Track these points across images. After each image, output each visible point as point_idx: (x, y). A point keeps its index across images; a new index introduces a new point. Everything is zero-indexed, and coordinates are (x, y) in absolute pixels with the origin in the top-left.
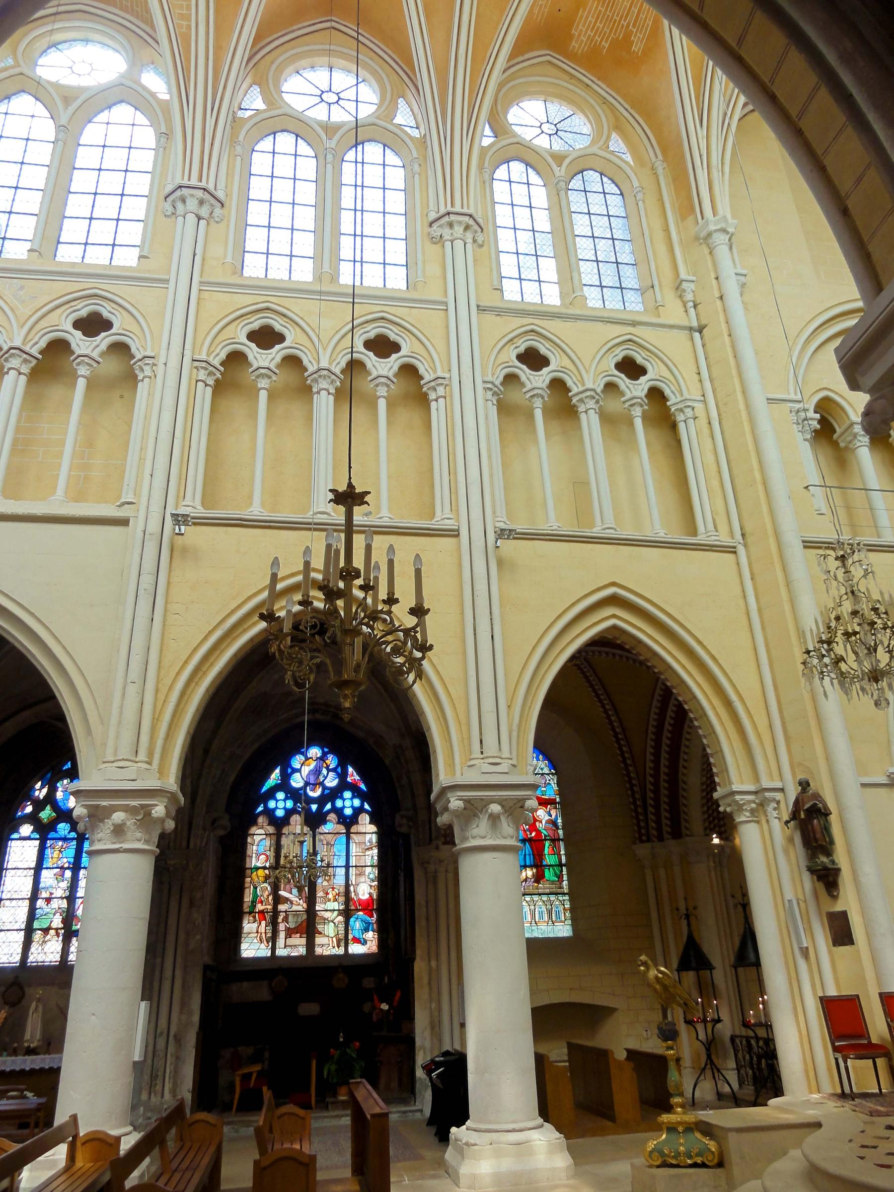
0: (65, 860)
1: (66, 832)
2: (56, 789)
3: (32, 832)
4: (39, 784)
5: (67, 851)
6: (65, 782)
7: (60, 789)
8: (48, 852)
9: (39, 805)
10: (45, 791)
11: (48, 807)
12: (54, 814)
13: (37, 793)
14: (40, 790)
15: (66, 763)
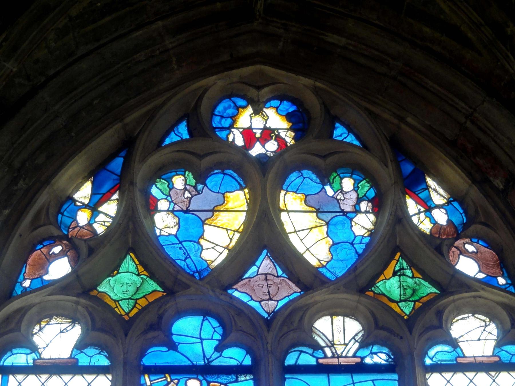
1: (209, 346)
2: (151, 206)
3: (81, 346)
4: (84, 193)
6: (178, 182)
7: (163, 205)
9: (94, 255)
10: (110, 208)
11: (129, 264)
12: (151, 286)
13: (83, 217)
14: (94, 208)
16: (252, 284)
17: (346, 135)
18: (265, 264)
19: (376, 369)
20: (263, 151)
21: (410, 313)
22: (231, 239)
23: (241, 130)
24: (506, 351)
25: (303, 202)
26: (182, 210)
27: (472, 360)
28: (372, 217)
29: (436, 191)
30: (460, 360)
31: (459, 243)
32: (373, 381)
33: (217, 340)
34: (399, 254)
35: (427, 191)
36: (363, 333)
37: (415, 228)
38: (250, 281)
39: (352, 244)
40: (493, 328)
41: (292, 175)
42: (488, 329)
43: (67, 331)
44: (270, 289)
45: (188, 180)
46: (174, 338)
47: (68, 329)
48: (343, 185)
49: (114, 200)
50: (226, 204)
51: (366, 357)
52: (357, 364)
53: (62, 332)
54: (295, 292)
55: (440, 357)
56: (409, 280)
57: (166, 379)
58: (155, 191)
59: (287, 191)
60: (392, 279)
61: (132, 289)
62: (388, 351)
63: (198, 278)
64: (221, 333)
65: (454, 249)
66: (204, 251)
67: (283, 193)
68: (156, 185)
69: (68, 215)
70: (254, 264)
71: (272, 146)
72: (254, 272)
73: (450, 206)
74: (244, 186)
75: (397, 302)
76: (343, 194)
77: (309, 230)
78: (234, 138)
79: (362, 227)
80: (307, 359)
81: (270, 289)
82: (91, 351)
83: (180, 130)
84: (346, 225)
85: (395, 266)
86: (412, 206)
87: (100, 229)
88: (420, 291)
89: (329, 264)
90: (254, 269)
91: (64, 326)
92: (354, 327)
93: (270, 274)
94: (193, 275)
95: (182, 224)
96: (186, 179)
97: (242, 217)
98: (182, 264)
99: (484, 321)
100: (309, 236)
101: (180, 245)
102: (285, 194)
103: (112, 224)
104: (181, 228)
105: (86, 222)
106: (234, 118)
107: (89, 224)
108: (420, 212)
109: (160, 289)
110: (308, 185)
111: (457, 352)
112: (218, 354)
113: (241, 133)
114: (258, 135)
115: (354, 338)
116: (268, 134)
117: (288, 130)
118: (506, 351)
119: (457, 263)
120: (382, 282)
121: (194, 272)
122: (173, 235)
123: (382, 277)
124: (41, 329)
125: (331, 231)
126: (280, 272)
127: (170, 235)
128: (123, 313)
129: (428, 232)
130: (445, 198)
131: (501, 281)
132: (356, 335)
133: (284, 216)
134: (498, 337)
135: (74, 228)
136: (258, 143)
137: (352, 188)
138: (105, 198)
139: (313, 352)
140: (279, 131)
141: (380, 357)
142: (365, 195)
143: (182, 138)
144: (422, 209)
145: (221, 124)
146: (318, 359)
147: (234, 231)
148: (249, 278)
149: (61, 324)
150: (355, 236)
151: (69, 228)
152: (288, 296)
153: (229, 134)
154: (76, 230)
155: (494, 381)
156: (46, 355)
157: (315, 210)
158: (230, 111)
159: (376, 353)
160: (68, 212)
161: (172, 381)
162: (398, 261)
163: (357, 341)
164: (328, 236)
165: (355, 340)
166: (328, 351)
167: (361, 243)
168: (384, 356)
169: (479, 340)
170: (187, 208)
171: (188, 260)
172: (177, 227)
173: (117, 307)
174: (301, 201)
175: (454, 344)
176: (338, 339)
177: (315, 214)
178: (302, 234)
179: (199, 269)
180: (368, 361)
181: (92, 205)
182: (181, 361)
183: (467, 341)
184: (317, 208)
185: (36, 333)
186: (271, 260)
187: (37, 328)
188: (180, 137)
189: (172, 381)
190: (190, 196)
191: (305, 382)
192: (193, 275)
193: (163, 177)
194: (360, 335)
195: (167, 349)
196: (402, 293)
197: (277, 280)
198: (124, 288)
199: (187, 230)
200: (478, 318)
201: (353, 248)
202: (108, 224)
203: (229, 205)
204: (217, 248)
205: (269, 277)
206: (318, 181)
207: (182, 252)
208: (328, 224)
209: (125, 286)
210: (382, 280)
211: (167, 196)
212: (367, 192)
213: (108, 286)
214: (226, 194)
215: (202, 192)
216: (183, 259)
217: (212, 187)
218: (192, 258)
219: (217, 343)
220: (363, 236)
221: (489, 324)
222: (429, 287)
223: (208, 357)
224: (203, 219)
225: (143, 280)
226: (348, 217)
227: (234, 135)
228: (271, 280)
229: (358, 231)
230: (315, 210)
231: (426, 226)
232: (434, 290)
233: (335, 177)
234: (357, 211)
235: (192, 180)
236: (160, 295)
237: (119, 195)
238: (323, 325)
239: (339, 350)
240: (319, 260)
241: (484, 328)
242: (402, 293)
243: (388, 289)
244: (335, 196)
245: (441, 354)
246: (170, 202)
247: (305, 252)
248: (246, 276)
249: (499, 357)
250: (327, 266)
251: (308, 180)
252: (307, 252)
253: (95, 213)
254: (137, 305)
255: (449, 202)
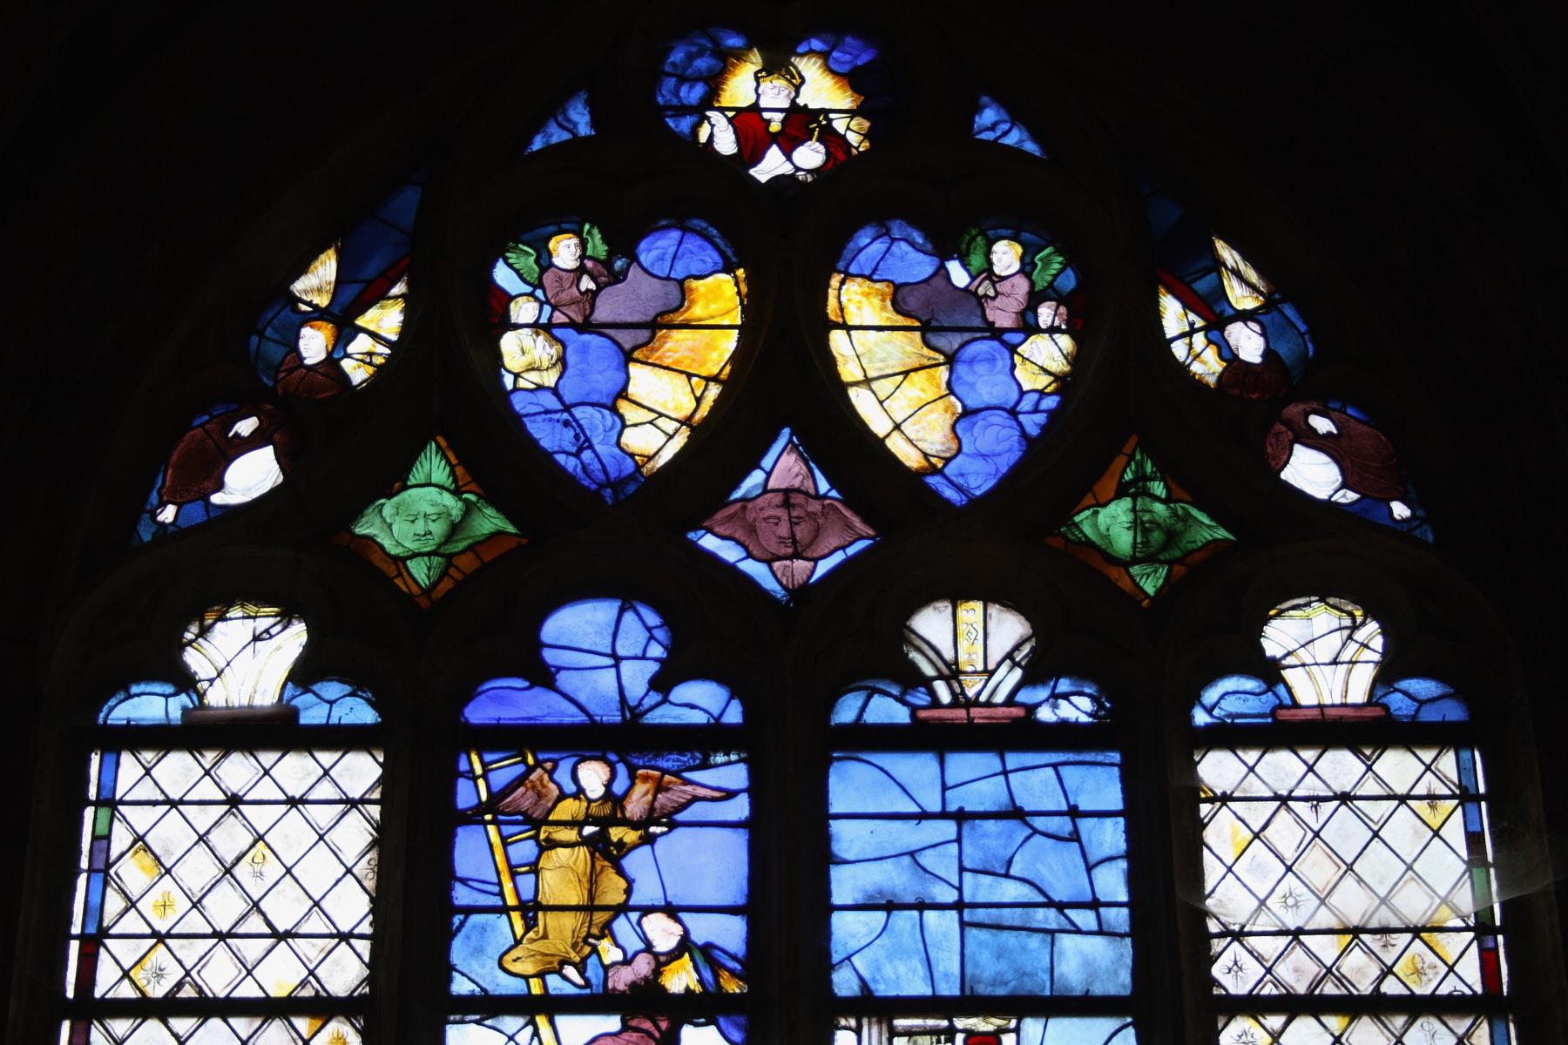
0: (663, 932)
1: (637, 677)
3: (304, 675)
4: (319, 279)
5: (675, 845)
6: (565, 251)
7: (524, 311)
8: (474, 853)
9: (344, 444)
10: (386, 319)
11: (433, 466)
12: (490, 521)
13: (314, 344)
15: (553, 109)
16: (750, 516)
17: (1006, 127)
18: (782, 465)
19: (1064, 737)
20: (787, 169)
21: (1158, 592)
22: (699, 400)
23: (730, 114)
24: (1405, 693)
25: (888, 303)
26: (572, 325)
27: (1316, 712)
28: (1066, 342)
29: (1237, 273)
30: (1284, 715)
31: (1293, 410)
32: (1055, 766)
33: (656, 660)
34: (1133, 440)
35: (1214, 275)
36: (1033, 642)
37: (1183, 369)
38: (744, 508)
39: (1013, 413)
40: (1371, 631)
41: (861, 233)
42: (1360, 635)
43: (271, 637)
44: (797, 529)
45: (589, 246)
46: (550, 656)
47: (273, 631)
48: (994, 258)
49: (396, 297)
50: (689, 308)
51: (1039, 705)
52: (1016, 720)
53: (256, 638)
54: (861, 538)
55: (1231, 705)
56: (1159, 508)
57: (524, 761)
58: (503, 276)
59: (848, 276)
60: (1113, 506)
61: (439, 529)
62: (1098, 691)
63: (609, 501)
64: (666, 641)
65: (1279, 427)
66: (627, 431)
67: (835, 281)
68: (506, 260)
69: (276, 336)
70: (757, 465)
71: (810, 156)
72: (755, 486)
73: (1275, 313)
74: (734, 259)
75: (1124, 564)
76: (994, 284)
77: (900, 378)
78: (711, 136)
79: (1042, 368)
80: (887, 710)
81: (797, 529)
82: (332, 689)
83: (573, 115)
84: (1000, 364)
85: (1124, 471)
86: (1173, 315)
87: (357, 373)
88: (1188, 537)
89: (953, 464)
90: (756, 477)
91: (263, 624)
92: (1009, 628)
93: (798, 491)
94: (597, 494)
95: (572, 359)
96: (583, 244)
97: (728, 342)
98: (570, 463)
99: (1351, 614)
100: (902, 396)
101: (565, 416)
102: (843, 283)
103: (389, 358)
104: (570, 372)
105: (323, 356)
106: (714, 83)
107: (331, 363)
108: (1193, 331)
109: (511, 529)
110: (902, 258)
111: (1275, 694)
112: (654, 698)
113: (730, 120)
114: (775, 127)
115: (1009, 656)
116: (802, 123)
117: (852, 113)
118: (1405, 693)
119: (1287, 462)
120: (1087, 513)
121: (601, 486)
122: (548, 388)
123: (1089, 500)
124: (204, 632)
125: (959, 378)
126: (823, 486)
127: (540, 388)
128: (415, 590)
129: (1211, 381)
130: (1261, 293)
131: (1400, 510)
132: (1017, 647)
133: (837, 339)
134: (1383, 654)
135: (291, 371)
136: (775, 148)
137: (1016, 266)
138: (375, 295)
139: (904, 693)
140: (832, 116)
141: (1078, 710)
142: (1051, 284)
143: (575, 135)
144: (1199, 323)
145: (679, 98)
146: (914, 709)
147: (708, 379)
148: (744, 499)
149: (255, 618)
150: (1022, 393)
151: (278, 370)
152: (843, 548)
153: (699, 124)
154: (297, 374)
155: (1369, 768)
156: (216, 697)
157: (917, 324)
158: (702, 64)
159: (1066, 696)
160: (276, 330)
161: (538, 764)
162: (1131, 457)
163: (1018, 664)
164: (951, 392)
165: (1012, 660)
166: (943, 692)
167: (1036, 410)
168: (1085, 703)
169: (1335, 662)
170: (587, 318)
171: (587, 455)
172: (559, 367)
173: (400, 575)
174: (883, 300)
175: (1270, 672)
176: (971, 656)
177: (918, 334)
178: (884, 387)
179: (613, 475)
180: (1045, 714)
181: (336, 310)
182: (563, 714)
183: (1303, 665)
184: (924, 318)
185: (190, 643)
186: (800, 454)
187: (194, 629)
188: (569, 131)
189: (538, 764)
190: (592, 286)
191: (882, 769)
192: (597, 494)
193: (525, 237)
194: (1026, 649)
195: (527, 684)
196: (1139, 540)
197: (815, 506)
198: (420, 527)
199: (583, 375)
200: (1333, 607)
201: (1014, 424)
202: (379, 360)
203: (697, 311)
204: (661, 422)
205: (797, 499)
206: (929, 247)
207: (569, 434)
208: (951, 360)
209: (421, 522)
210: (1088, 508)
211: (535, 287)
212: (1055, 276)
213: (378, 521)
214: (687, 283)
215: (625, 278)
216: (574, 449)
217: (653, 264)
218: (598, 448)
219: (653, 667)
220: (1042, 393)
221: (1363, 624)
222: (1209, 527)
223: (633, 703)
224: (627, 346)
225: (469, 508)
226: (1004, 344)
227: (713, 126)
228: (800, 505)
229: (1030, 379)
230: (917, 324)
231: (1208, 366)
232: (1221, 533)
233: (973, 239)
234: (1028, 327)
235: (598, 247)
236: (513, 544)
237: (409, 285)
238: (932, 624)
239: (972, 687)
240: (926, 455)
241: (1346, 633)
242: (1139, 540)
243: (1102, 528)
244: (972, 288)
245: (1232, 698)
246: (542, 304)
247: (888, 435)
248: (737, 494)
249: (1386, 707)
250: (947, 471)
251: (903, 245)
252: (896, 434)
253: (346, 330)
254: (452, 571)
255: (1269, 306)
